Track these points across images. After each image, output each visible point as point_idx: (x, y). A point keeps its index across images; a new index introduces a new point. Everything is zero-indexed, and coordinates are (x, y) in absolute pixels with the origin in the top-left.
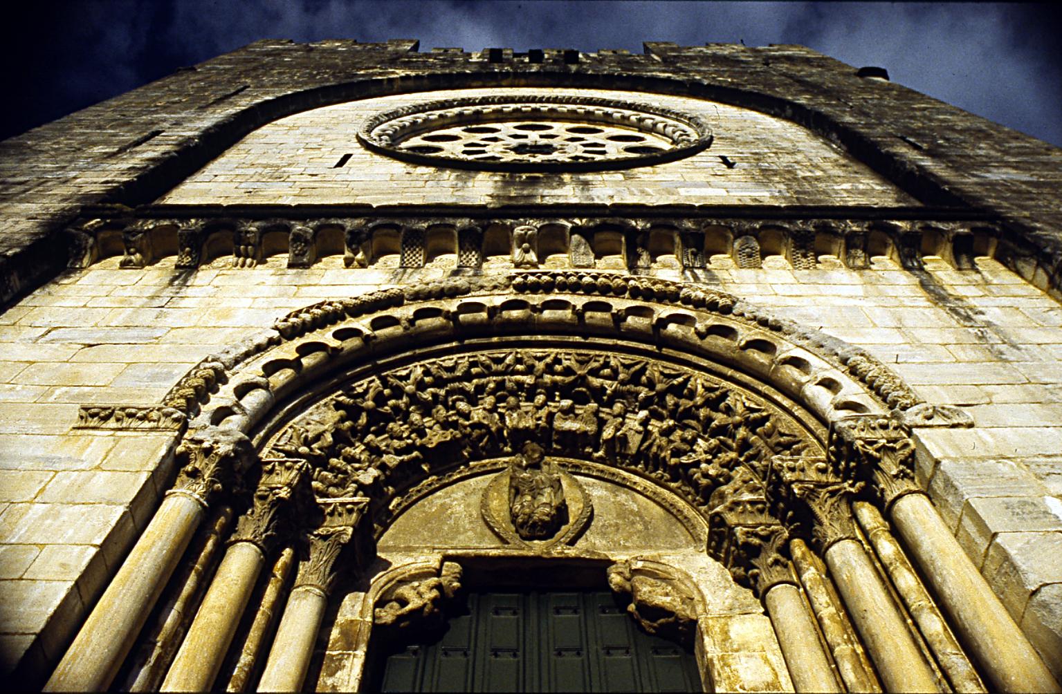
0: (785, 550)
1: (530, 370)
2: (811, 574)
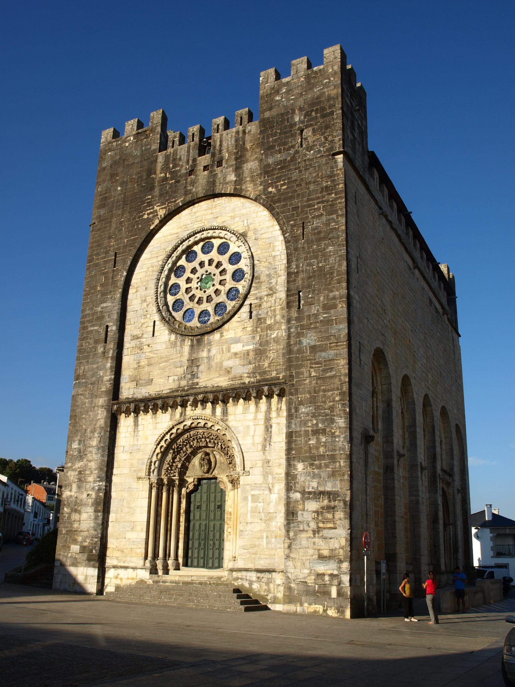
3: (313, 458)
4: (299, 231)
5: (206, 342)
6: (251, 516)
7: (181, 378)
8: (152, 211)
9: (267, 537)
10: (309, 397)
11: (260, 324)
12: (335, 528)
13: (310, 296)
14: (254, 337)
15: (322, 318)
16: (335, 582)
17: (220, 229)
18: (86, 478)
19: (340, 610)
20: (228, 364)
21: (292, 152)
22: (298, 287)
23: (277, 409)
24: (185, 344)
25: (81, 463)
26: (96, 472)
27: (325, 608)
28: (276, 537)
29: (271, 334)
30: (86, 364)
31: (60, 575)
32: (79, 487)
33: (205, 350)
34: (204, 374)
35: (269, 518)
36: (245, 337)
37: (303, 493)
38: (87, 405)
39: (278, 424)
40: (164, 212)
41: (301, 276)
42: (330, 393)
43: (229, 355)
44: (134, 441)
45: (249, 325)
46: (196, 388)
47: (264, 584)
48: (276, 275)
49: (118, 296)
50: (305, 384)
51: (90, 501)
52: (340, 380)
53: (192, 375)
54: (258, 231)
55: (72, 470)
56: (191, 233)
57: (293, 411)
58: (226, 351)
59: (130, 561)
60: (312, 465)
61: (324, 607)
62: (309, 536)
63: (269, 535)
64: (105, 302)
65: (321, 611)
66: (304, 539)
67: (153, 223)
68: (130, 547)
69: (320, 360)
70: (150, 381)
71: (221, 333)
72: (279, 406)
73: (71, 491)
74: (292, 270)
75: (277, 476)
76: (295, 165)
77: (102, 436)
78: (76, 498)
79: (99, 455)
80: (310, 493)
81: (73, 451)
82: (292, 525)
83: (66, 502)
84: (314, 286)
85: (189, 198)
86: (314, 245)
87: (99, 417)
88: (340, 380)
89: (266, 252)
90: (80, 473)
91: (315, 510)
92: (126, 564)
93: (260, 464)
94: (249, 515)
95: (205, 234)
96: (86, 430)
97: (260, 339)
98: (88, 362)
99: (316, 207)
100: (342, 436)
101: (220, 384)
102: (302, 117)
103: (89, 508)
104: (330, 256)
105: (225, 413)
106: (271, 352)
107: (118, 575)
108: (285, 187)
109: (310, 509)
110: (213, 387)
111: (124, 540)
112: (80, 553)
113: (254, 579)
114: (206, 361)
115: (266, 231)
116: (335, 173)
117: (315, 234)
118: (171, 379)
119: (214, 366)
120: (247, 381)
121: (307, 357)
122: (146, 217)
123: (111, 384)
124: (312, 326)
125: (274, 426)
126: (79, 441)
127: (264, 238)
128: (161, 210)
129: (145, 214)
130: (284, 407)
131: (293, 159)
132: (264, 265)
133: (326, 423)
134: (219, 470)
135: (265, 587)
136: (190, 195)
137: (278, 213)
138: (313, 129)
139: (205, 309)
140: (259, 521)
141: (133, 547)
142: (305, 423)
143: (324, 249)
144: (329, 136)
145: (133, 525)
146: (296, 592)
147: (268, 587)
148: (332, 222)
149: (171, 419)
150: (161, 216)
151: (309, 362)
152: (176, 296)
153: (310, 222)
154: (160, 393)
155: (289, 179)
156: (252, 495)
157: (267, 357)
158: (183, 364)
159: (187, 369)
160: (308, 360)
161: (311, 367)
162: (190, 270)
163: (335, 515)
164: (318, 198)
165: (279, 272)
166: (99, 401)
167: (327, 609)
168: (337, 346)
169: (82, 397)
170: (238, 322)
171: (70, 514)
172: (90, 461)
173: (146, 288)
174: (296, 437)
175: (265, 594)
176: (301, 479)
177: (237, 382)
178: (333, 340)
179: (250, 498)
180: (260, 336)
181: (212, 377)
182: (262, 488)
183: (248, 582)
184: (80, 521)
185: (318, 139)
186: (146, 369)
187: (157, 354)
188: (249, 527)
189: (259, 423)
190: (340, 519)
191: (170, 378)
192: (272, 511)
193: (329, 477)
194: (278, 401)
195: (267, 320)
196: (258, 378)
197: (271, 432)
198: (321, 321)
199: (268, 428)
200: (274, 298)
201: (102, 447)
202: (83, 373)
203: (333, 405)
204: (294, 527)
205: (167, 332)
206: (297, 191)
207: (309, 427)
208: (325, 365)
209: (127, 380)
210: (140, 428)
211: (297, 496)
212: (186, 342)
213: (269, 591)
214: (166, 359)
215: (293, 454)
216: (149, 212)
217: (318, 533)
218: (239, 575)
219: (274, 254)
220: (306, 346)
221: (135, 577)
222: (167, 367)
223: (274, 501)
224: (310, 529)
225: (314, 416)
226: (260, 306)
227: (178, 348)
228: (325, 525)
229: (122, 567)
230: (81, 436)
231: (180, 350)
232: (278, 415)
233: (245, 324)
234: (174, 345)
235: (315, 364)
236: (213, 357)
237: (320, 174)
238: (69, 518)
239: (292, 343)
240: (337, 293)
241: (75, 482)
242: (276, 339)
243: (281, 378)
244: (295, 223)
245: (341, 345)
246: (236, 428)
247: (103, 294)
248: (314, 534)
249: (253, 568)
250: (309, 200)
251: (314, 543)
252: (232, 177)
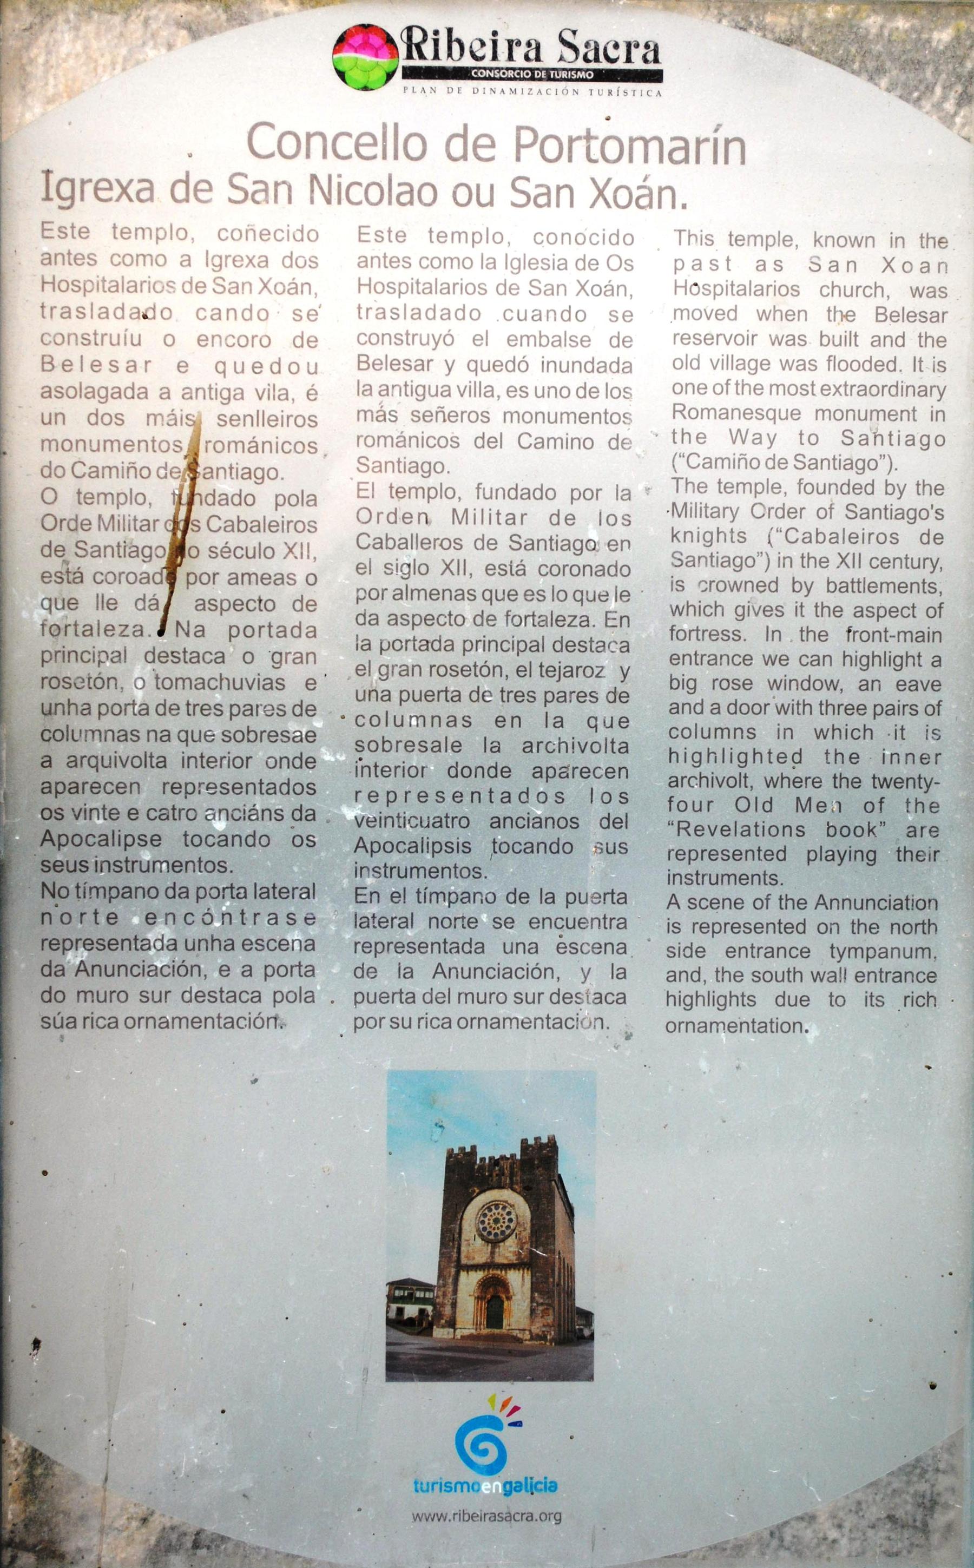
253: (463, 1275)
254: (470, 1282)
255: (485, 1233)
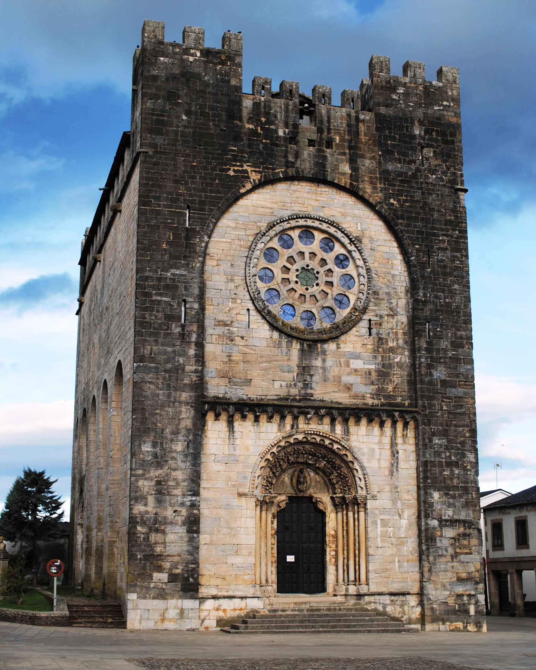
0: (342, 505)
1: (304, 450)
2: (345, 512)
3: (448, 488)
4: (425, 259)
5: (319, 350)
6: (382, 541)
7: (291, 385)
8: (240, 169)
9: (399, 561)
10: (441, 429)
11: (382, 344)
12: (471, 554)
13: (438, 329)
14: (376, 356)
15: (450, 355)
16: (473, 601)
17: (329, 224)
18: (170, 490)
19: (478, 625)
20: (347, 379)
21: (413, 167)
22: (426, 316)
23: (403, 435)
24: (293, 347)
25: (160, 471)
26: (186, 484)
27: (465, 625)
28: (408, 561)
29: (394, 358)
30: (153, 343)
31: (139, 611)
32: (159, 502)
33: (319, 359)
34: (319, 385)
35: (401, 543)
36: (365, 354)
37: (440, 521)
38: (161, 397)
39: (405, 450)
40: (259, 177)
41: (431, 306)
42: (461, 429)
43: (348, 370)
44: (229, 450)
45: (370, 342)
46: (310, 399)
47: (398, 607)
48: (397, 296)
49: (198, 265)
50: (437, 416)
51: (179, 519)
52: (470, 418)
53: (304, 384)
54: (373, 240)
55: (145, 479)
56: (293, 215)
57: (427, 441)
58: (344, 365)
59: (236, 589)
60: (447, 494)
61: (464, 624)
62: (447, 560)
63: (401, 559)
64: (177, 268)
65: (462, 628)
66: (442, 564)
67: (244, 186)
68: (234, 573)
69: (451, 395)
70: (249, 382)
71: (337, 344)
72: (405, 433)
73: (146, 505)
74: (420, 298)
75: (406, 502)
76: (417, 183)
77: (190, 441)
78: (156, 514)
79: (188, 464)
80: (446, 521)
81: (143, 454)
82: (431, 550)
83: (138, 520)
84: (442, 321)
85: (291, 172)
86: (441, 278)
87: (183, 415)
88: (470, 418)
89: (384, 268)
90: (158, 483)
91: (452, 536)
92: (231, 593)
93: (387, 488)
94: (379, 539)
95: (309, 223)
96: (163, 430)
97: (382, 361)
98: (156, 341)
99: (441, 238)
100: (473, 470)
101: (340, 401)
102: (423, 133)
103: (178, 527)
104: (456, 294)
105: (347, 432)
106: (395, 376)
107: (220, 606)
108: (407, 204)
109: (447, 536)
110: (332, 402)
111: (225, 565)
112: (169, 582)
113: (388, 602)
114: (320, 371)
115: (383, 244)
116: (458, 209)
117: (441, 266)
118: (277, 384)
119: (331, 379)
120: (370, 401)
121: (438, 390)
122: (231, 173)
123: (198, 376)
124: (442, 360)
125: (401, 452)
126: (153, 442)
127: (381, 252)
128: (254, 173)
129: (230, 169)
130: (411, 433)
131: (414, 176)
132: (382, 281)
133: (458, 457)
134: (315, 489)
135: (399, 609)
136: (294, 169)
137: (402, 231)
138: (435, 152)
139: (309, 309)
140: (390, 545)
141: (239, 573)
142: (438, 454)
143: (451, 286)
144: (451, 166)
145: (236, 548)
146: (438, 612)
147: (403, 609)
148: (457, 260)
149: (280, 430)
150: (254, 180)
151: (440, 395)
152: (269, 284)
153: (435, 253)
154: (263, 397)
155: (411, 196)
156: (381, 519)
157: (391, 380)
158: (292, 370)
159: (297, 376)
160: (439, 393)
161: (443, 401)
162: (285, 258)
163: (471, 542)
164: (443, 230)
165: (399, 294)
166: (180, 395)
167: (467, 626)
168: (466, 385)
169: (152, 387)
170: (356, 336)
171: (147, 535)
172: (175, 470)
173: (232, 265)
174: (431, 466)
175: (400, 616)
176: (438, 507)
177: (359, 401)
178: (461, 378)
179: (379, 522)
180: (382, 357)
181: (330, 390)
182: (391, 514)
183: (381, 605)
184: (164, 543)
185: (440, 165)
186: (241, 365)
187: (254, 350)
188: (380, 551)
189: (385, 448)
190: (475, 546)
191: (275, 382)
192: (403, 536)
193: (463, 507)
194: (404, 427)
195: (389, 342)
196: (382, 400)
197: (397, 458)
198: (450, 358)
199: (394, 454)
200: (395, 320)
201: (192, 453)
202: (151, 354)
203: (464, 440)
204: (433, 552)
205: (266, 327)
206: (421, 214)
207: (442, 458)
208: (455, 402)
209: (214, 374)
210: (236, 434)
211: (435, 523)
212: (294, 344)
213: (404, 613)
214: (268, 359)
215: (429, 483)
216: (236, 168)
217: (456, 558)
218: (372, 598)
219: (392, 272)
220: (436, 379)
221: (243, 608)
222: (270, 368)
223: (404, 526)
224: (449, 553)
225: (447, 448)
226: (380, 324)
227: (284, 350)
228: (461, 551)
229: (225, 597)
230: (155, 437)
231: (287, 353)
232: (404, 442)
233: (365, 340)
234: (279, 345)
235: (446, 399)
236: (329, 368)
237: (443, 205)
238: (147, 539)
239: (423, 373)
240: (464, 333)
241: (152, 494)
242: (399, 364)
243: (406, 405)
244: (420, 248)
245: (469, 385)
246: (360, 449)
247: (172, 257)
248: (452, 559)
249: (387, 592)
250: (433, 228)
251: (453, 567)
252: (346, 168)
253: (215, 429)
254: (239, 452)
255: (275, 308)
